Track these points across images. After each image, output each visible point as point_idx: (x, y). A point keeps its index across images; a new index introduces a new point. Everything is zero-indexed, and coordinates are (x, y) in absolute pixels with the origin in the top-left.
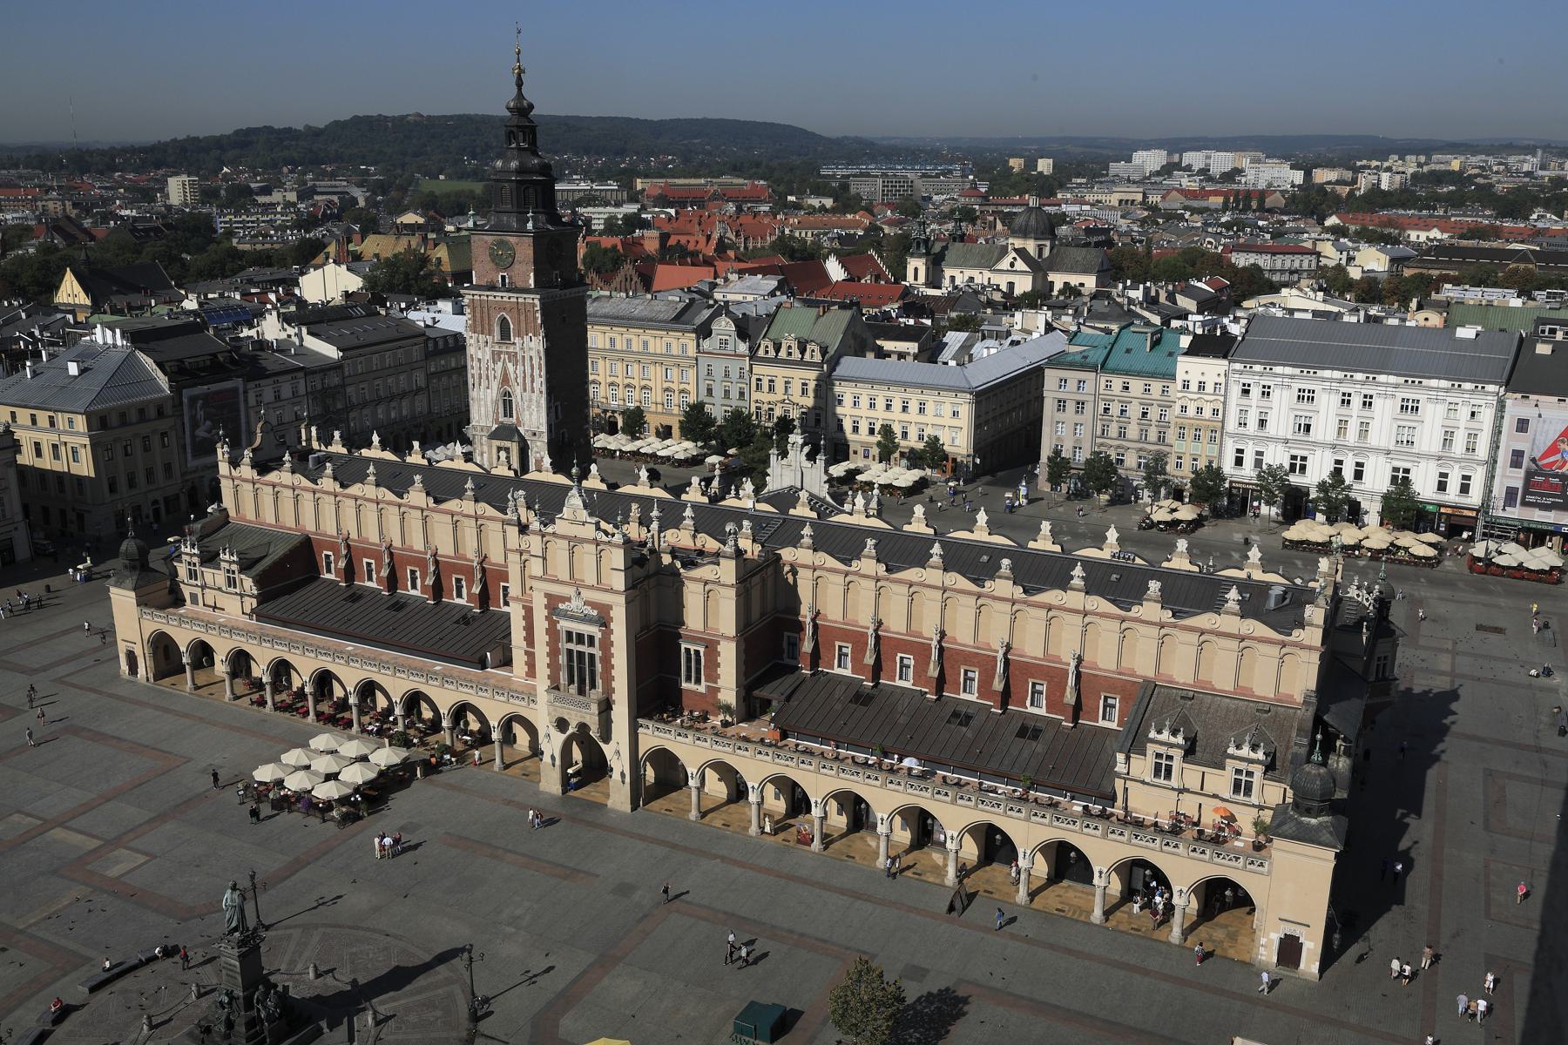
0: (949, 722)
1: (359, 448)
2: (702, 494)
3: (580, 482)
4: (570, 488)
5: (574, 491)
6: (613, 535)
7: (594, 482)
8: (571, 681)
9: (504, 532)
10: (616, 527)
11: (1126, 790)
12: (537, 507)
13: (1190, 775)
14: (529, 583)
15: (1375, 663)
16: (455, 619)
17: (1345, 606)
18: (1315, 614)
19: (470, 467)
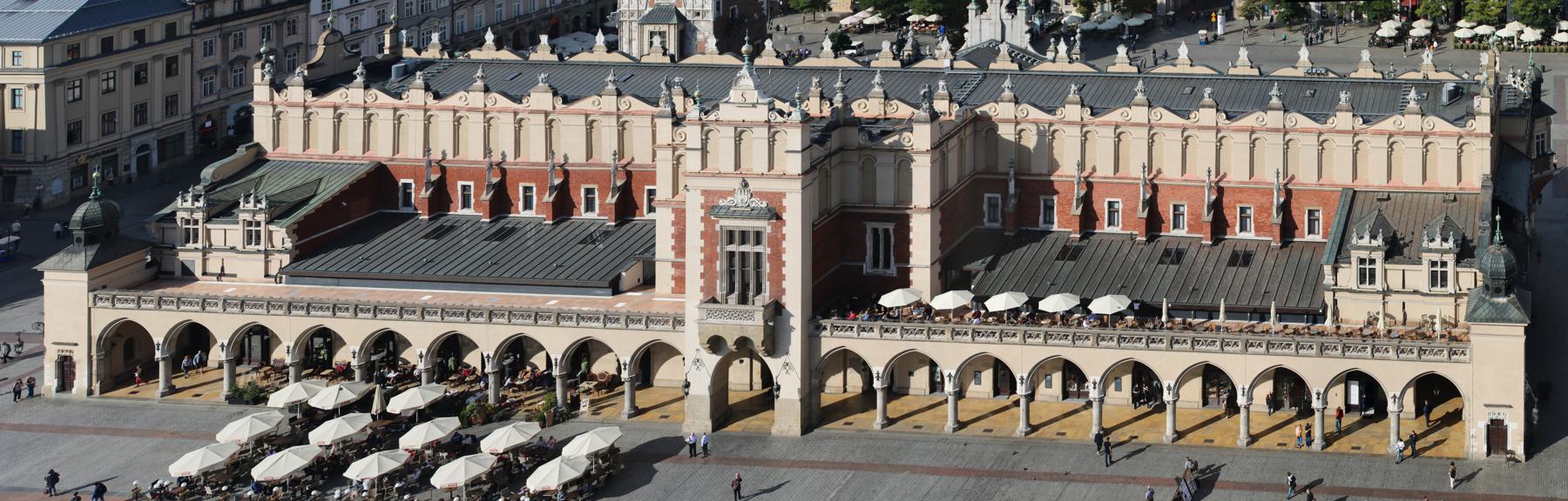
0: (1161, 262)
1: (466, 49)
2: (894, 59)
3: (751, 60)
4: (740, 68)
5: (744, 72)
6: (789, 114)
7: (768, 59)
8: (731, 291)
9: (654, 126)
10: (793, 104)
11: (1335, 302)
12: (696, 94)
13: (1395, 273)
14: (682, 181)
15: (1535, 141)
16: (580, 239)
17: (1505, 92)
18: (1483, 104)
19: (615, 57)
